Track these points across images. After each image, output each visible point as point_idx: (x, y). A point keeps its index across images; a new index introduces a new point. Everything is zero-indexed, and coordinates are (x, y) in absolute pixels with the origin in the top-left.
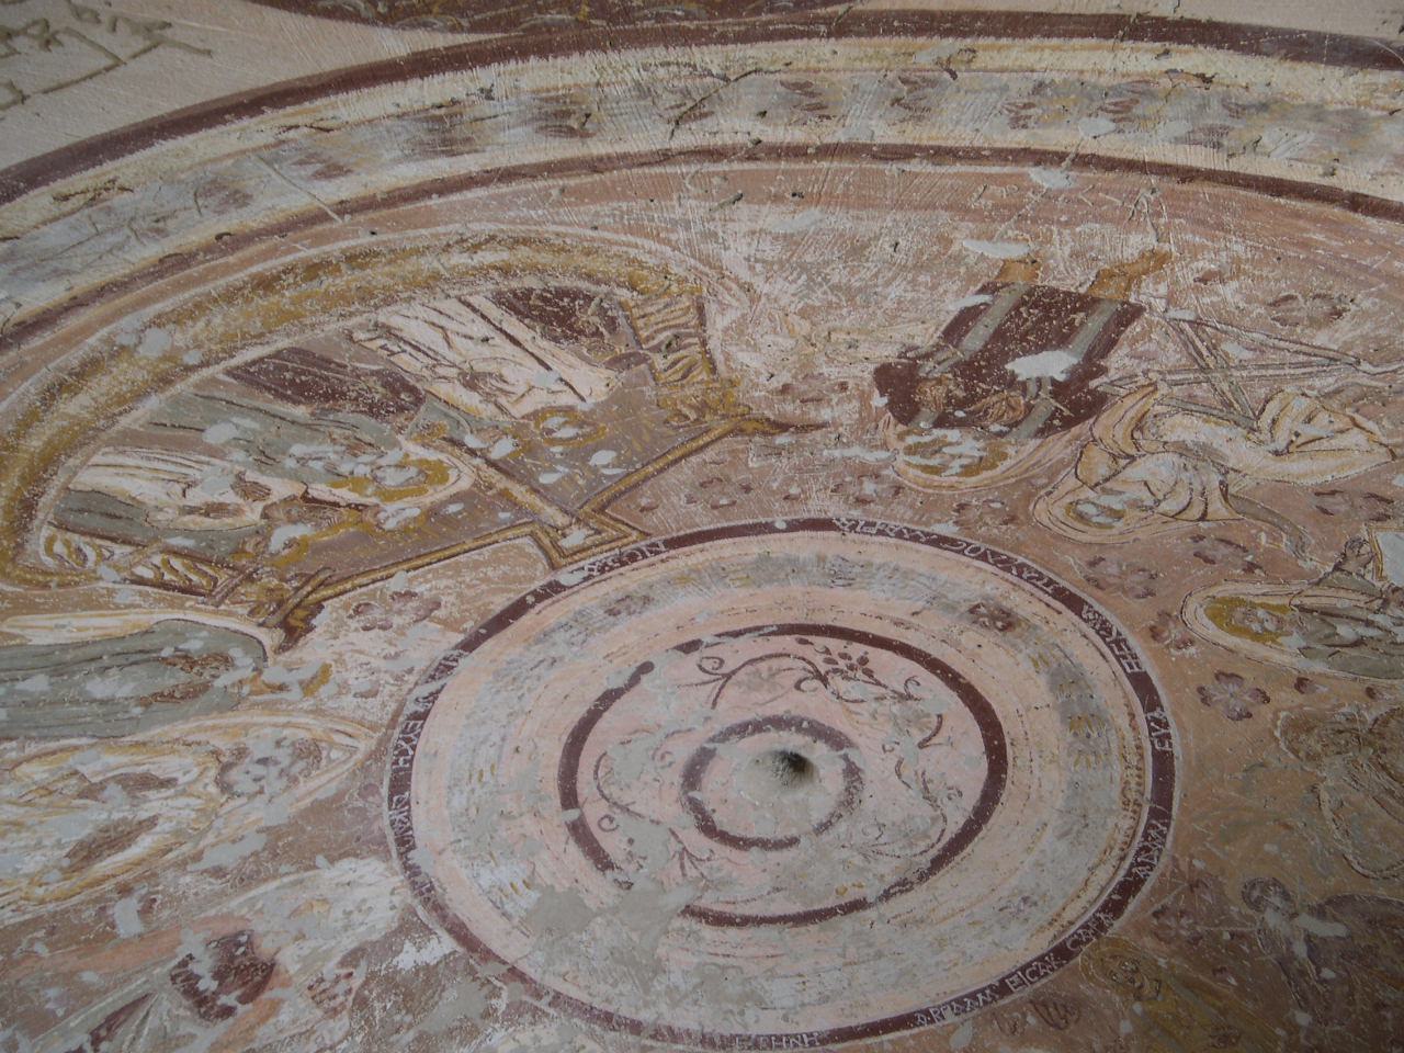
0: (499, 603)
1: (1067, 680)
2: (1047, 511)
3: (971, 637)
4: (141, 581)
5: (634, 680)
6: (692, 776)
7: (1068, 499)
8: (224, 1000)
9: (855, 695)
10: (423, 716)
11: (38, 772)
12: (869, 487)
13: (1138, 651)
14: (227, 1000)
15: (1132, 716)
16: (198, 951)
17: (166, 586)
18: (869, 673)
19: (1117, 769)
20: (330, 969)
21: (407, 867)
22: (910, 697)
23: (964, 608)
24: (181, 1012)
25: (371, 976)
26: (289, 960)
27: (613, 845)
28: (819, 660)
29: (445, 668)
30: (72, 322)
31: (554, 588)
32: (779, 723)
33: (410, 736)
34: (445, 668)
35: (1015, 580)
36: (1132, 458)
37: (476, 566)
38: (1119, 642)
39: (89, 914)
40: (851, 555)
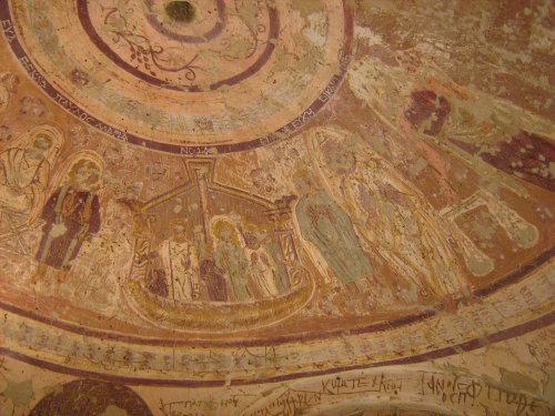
0: (237, 156)
1: (50, 45)
2: (58, 141)
3: (87, 66)
4: (296, 256)
5: (220, 83)
6: (218, 28)
7: (51, 149)
8: (438, 106)
9: (139, 40)
10: (290, 126)
11: (371, 236)
12: (113, 156)
13: (23, 69)
14: (437, 103)
15: (22, 34)
16: (421, 130)
17: (294, 249)
18: (132, 49)
19: (25, 5)
20: (401, 69)
21: (344, 72)
22: (118, 33)
23: (90, 83)
24: (450, 120)
25: (394, 49)
26: (407, 88)
27: (265, 19)
28: (150, 62)
29: (271, 139)
30: (233, 340)
31: (222, 149)
32: (175, 37)
33: (298, 121)
34: (271, 139)
35: (71, 99)
36: (33, 182)
37: (232, 180)
38: (30, 71)
39: (422, 182)
40: (126, 118)
